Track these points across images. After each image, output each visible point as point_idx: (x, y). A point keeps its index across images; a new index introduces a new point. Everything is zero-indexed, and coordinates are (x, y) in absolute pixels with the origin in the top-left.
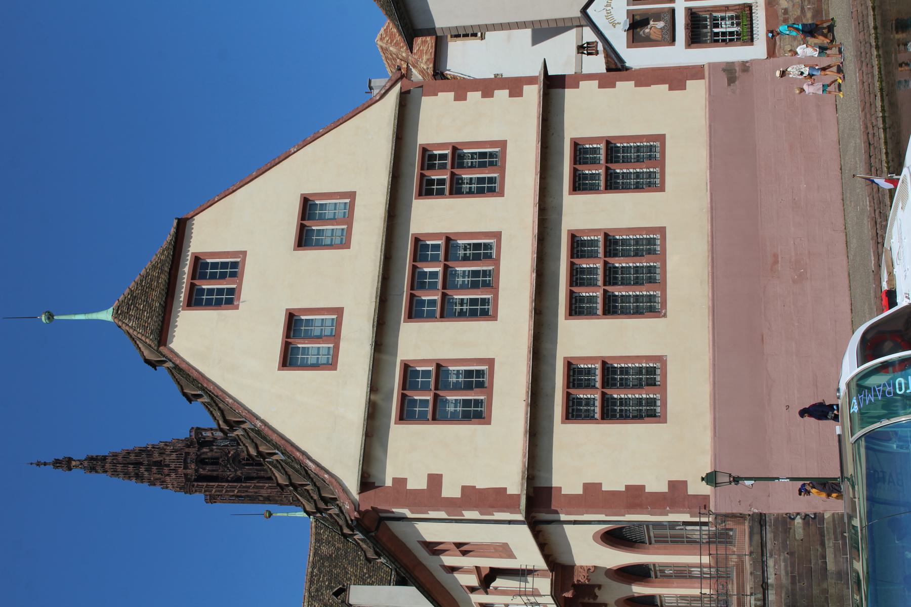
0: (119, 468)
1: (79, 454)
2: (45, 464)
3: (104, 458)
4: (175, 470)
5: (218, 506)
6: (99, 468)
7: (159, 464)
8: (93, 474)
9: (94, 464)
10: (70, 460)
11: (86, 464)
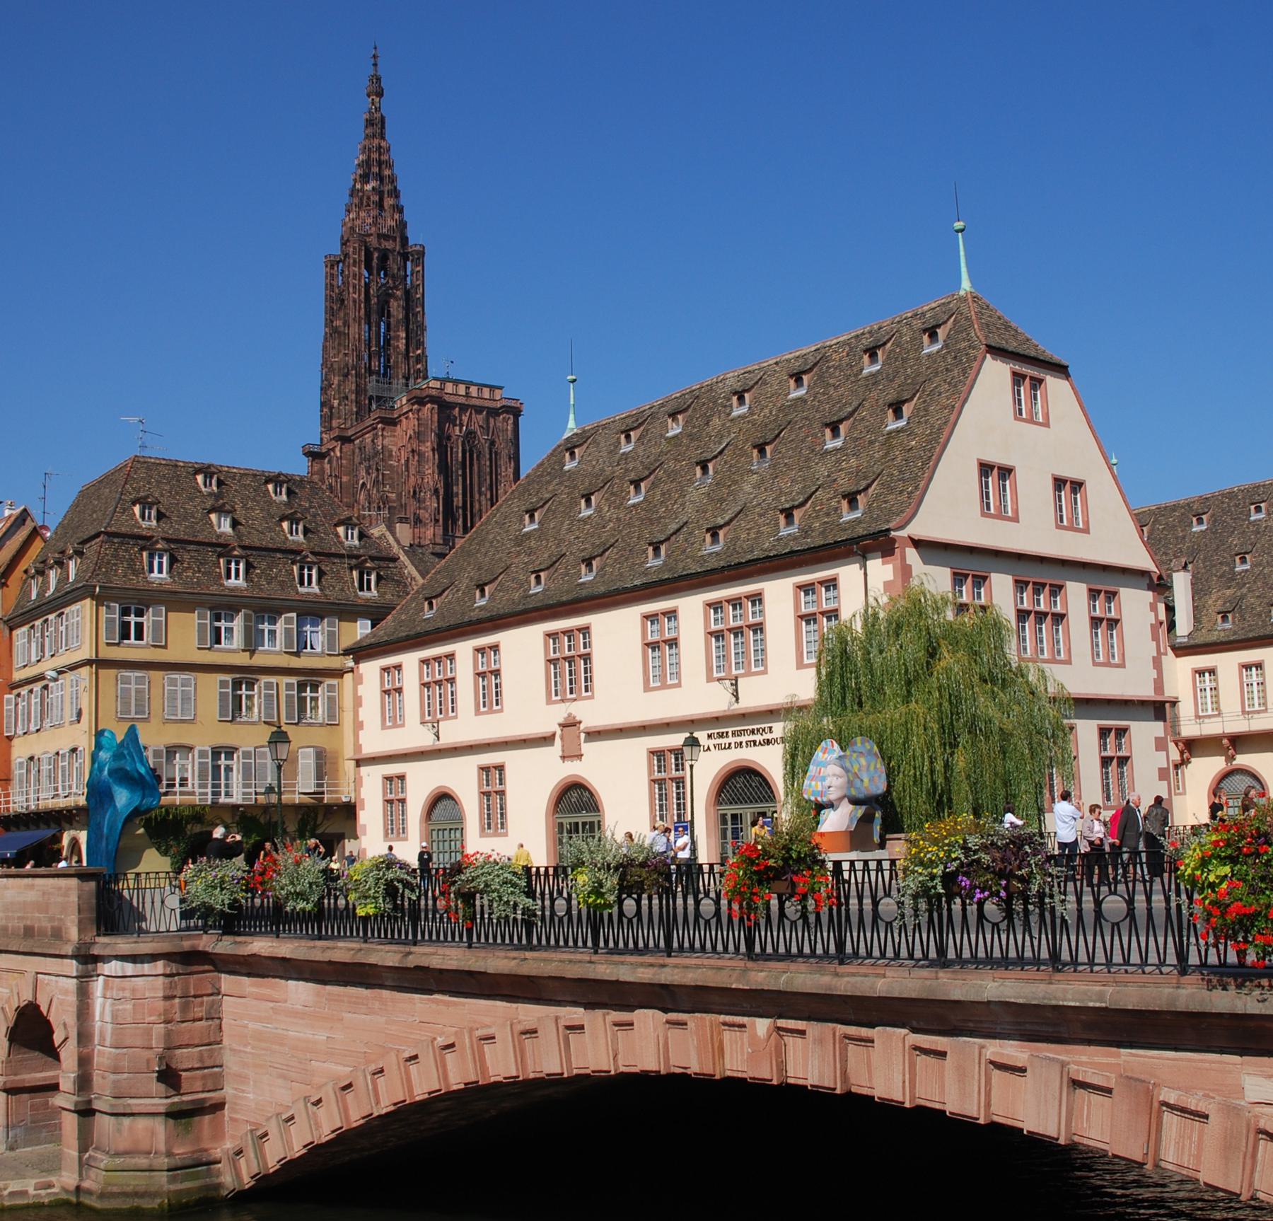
0: (375, 156)
1: (388, 107)
2: (375, 65)
3: (383, 138)
4: (375, 224)
5: (323, 270)
6: (369, 131)
7: (380, 205)
8: (363, 124)
9: (376, 125)
10: (380, 94)
11: (378, 115)
